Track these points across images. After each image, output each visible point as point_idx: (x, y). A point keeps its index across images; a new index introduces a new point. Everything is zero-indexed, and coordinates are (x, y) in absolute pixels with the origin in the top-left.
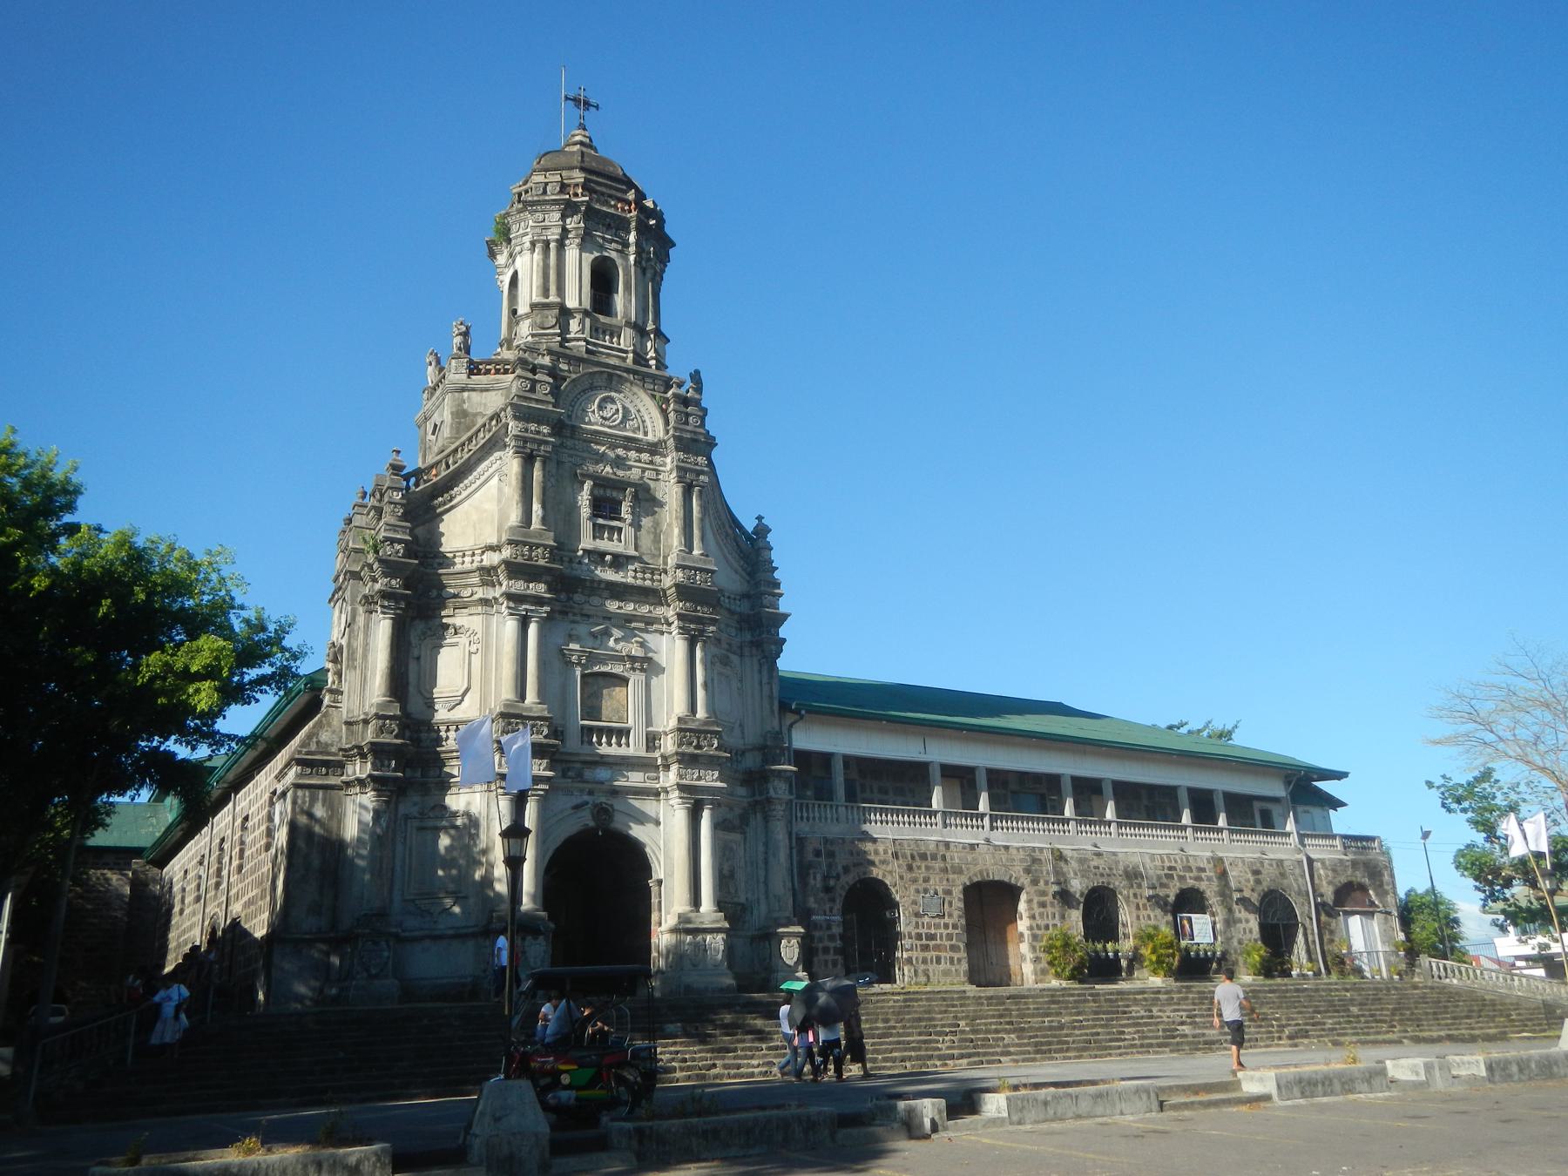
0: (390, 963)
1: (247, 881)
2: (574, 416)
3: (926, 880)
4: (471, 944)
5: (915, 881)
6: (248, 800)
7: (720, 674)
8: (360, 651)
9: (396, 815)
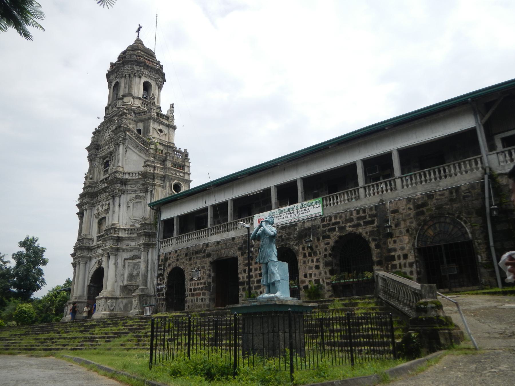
3: (196, 263)
5: (191, 265)
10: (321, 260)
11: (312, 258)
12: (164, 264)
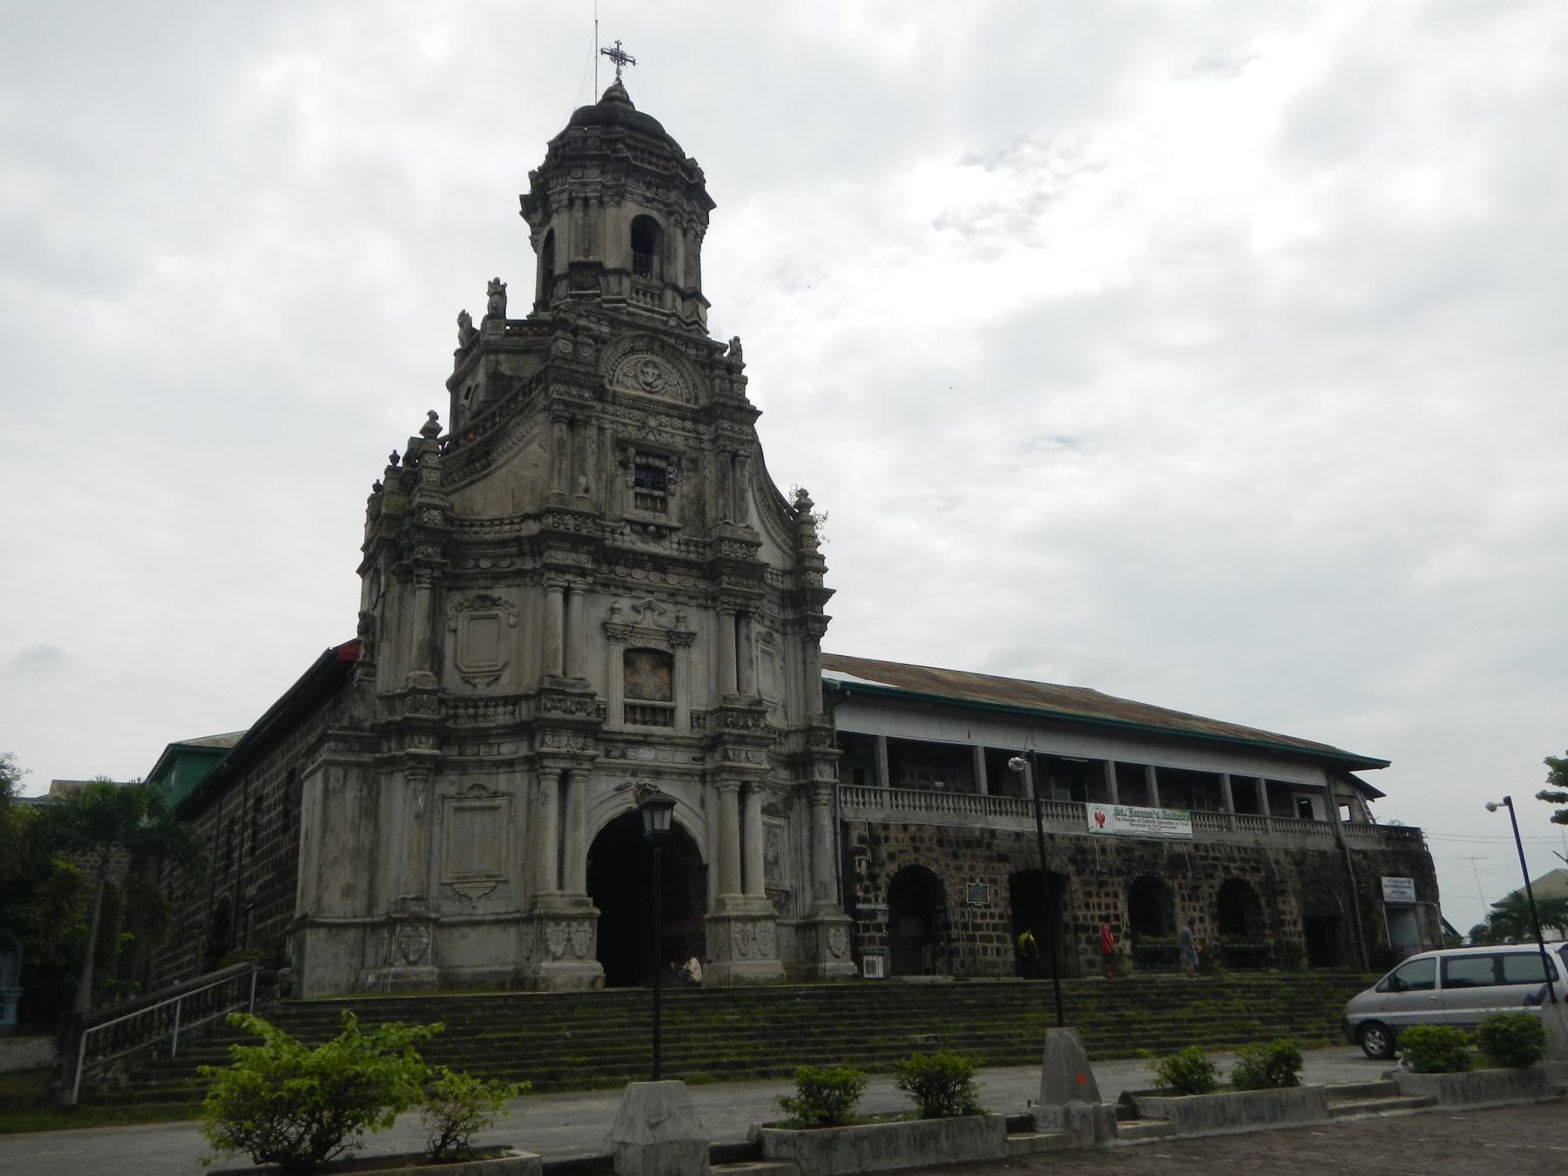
0: (430, 951)
1: (261, 864)
2: (615, 381)
3: (972, 868)
4: (512, 930)
5: (959, 869)
6: (261, 780)
7: (764, 652)
8: (395, 622)
9: (433, 794)
10: (1205, 909)
11: (1193, 904)
12: (873, 852)
